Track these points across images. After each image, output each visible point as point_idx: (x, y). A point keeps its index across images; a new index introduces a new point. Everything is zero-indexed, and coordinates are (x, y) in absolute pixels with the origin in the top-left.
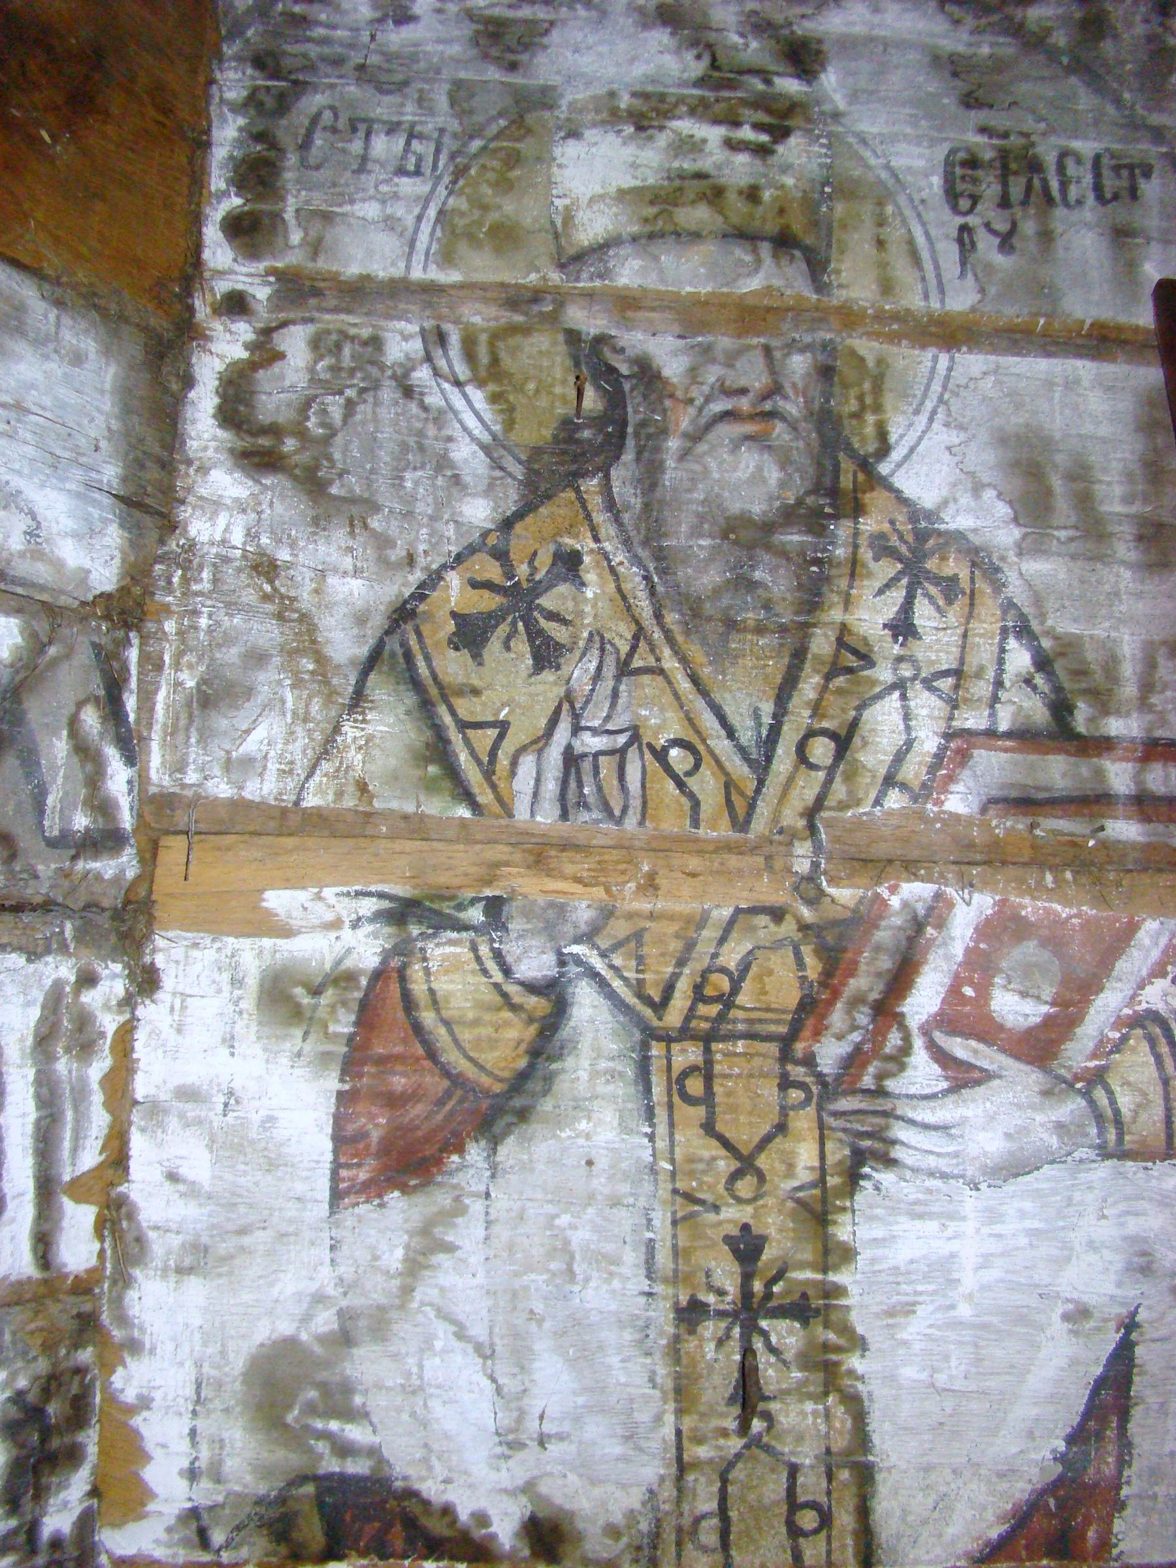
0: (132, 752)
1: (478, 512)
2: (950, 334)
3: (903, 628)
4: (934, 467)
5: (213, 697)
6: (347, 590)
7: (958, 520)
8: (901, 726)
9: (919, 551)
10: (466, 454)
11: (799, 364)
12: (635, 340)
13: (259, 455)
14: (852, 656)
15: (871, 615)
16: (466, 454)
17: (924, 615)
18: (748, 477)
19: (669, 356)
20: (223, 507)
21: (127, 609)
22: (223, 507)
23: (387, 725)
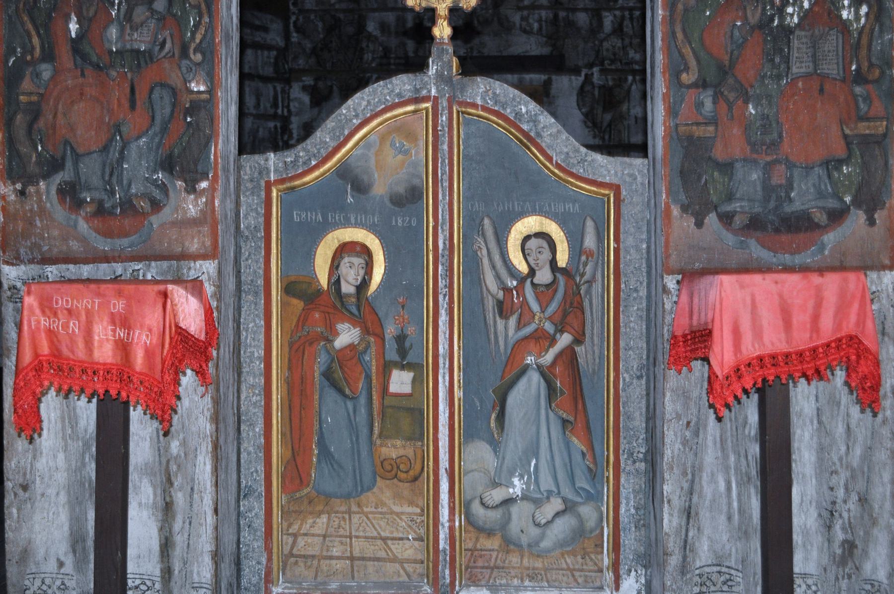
0: (288, 63)
1: (321, 36)
2: (374, 10)
3: (368, 46)
4: (371, 27)
5: (296, 58)
6: (308, 45)
7: (375, 33)
8: (368, 56)
9: (370, 37)
10: (320, 30)
11: (356, 16)
12: (338, 15)
13: (298, 30)
14: (362, 49)
15: (364, 45)
16: (320, 30)
17: (370, 45)
18: (350, 30)
19: (341, 16)
20: (295, 37)
21: (286, 48)
22: (295, 37)
23: (312, 61)
